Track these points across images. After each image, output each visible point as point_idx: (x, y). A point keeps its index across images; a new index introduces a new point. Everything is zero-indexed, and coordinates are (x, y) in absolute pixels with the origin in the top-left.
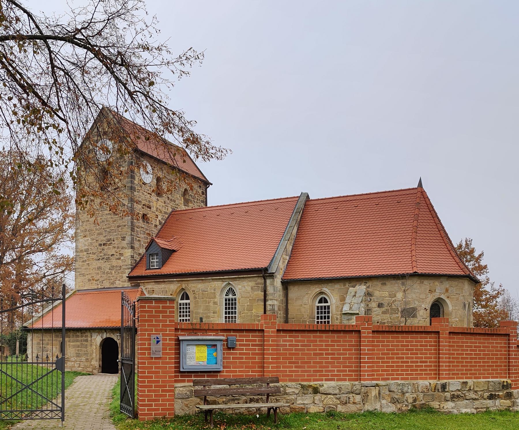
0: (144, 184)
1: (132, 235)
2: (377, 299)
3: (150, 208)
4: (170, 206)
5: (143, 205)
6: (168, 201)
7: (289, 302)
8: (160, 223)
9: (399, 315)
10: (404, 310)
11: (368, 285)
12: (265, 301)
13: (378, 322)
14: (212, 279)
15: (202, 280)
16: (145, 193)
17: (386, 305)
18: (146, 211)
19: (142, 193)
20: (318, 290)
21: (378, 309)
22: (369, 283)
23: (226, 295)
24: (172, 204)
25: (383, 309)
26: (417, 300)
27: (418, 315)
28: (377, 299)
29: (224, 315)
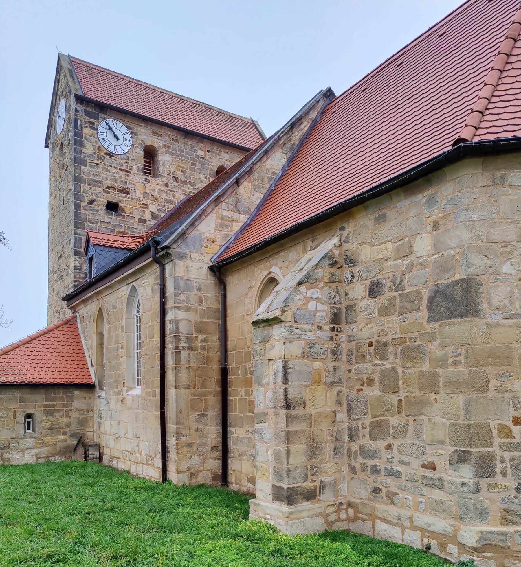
0: (109, 154)
1: (75, 234)
2: (368, 271)
3: (127, 193)
4: (180, 191)
5: (108, 187)
6: (176, 184)
7: (229, 311)
8: (153, 216)
9: (424, 312)
10: (436, 292)
11: (345, 233)
12: (163, 313)
13: (370, 345)
14: (117, 281)
15: (110, 287)
16: (113, 170)
17: (388, 285)
18: (114, 197)
19: (104, 168)
20: (265, 273)
21: (367, 301)
22: (350, 227)
23: (138, 312)
24: (185, 189)
25: (381, 301)
26: (478, 250)
27: (484, 306)
28: (368, 271)
29: (136, 351)
